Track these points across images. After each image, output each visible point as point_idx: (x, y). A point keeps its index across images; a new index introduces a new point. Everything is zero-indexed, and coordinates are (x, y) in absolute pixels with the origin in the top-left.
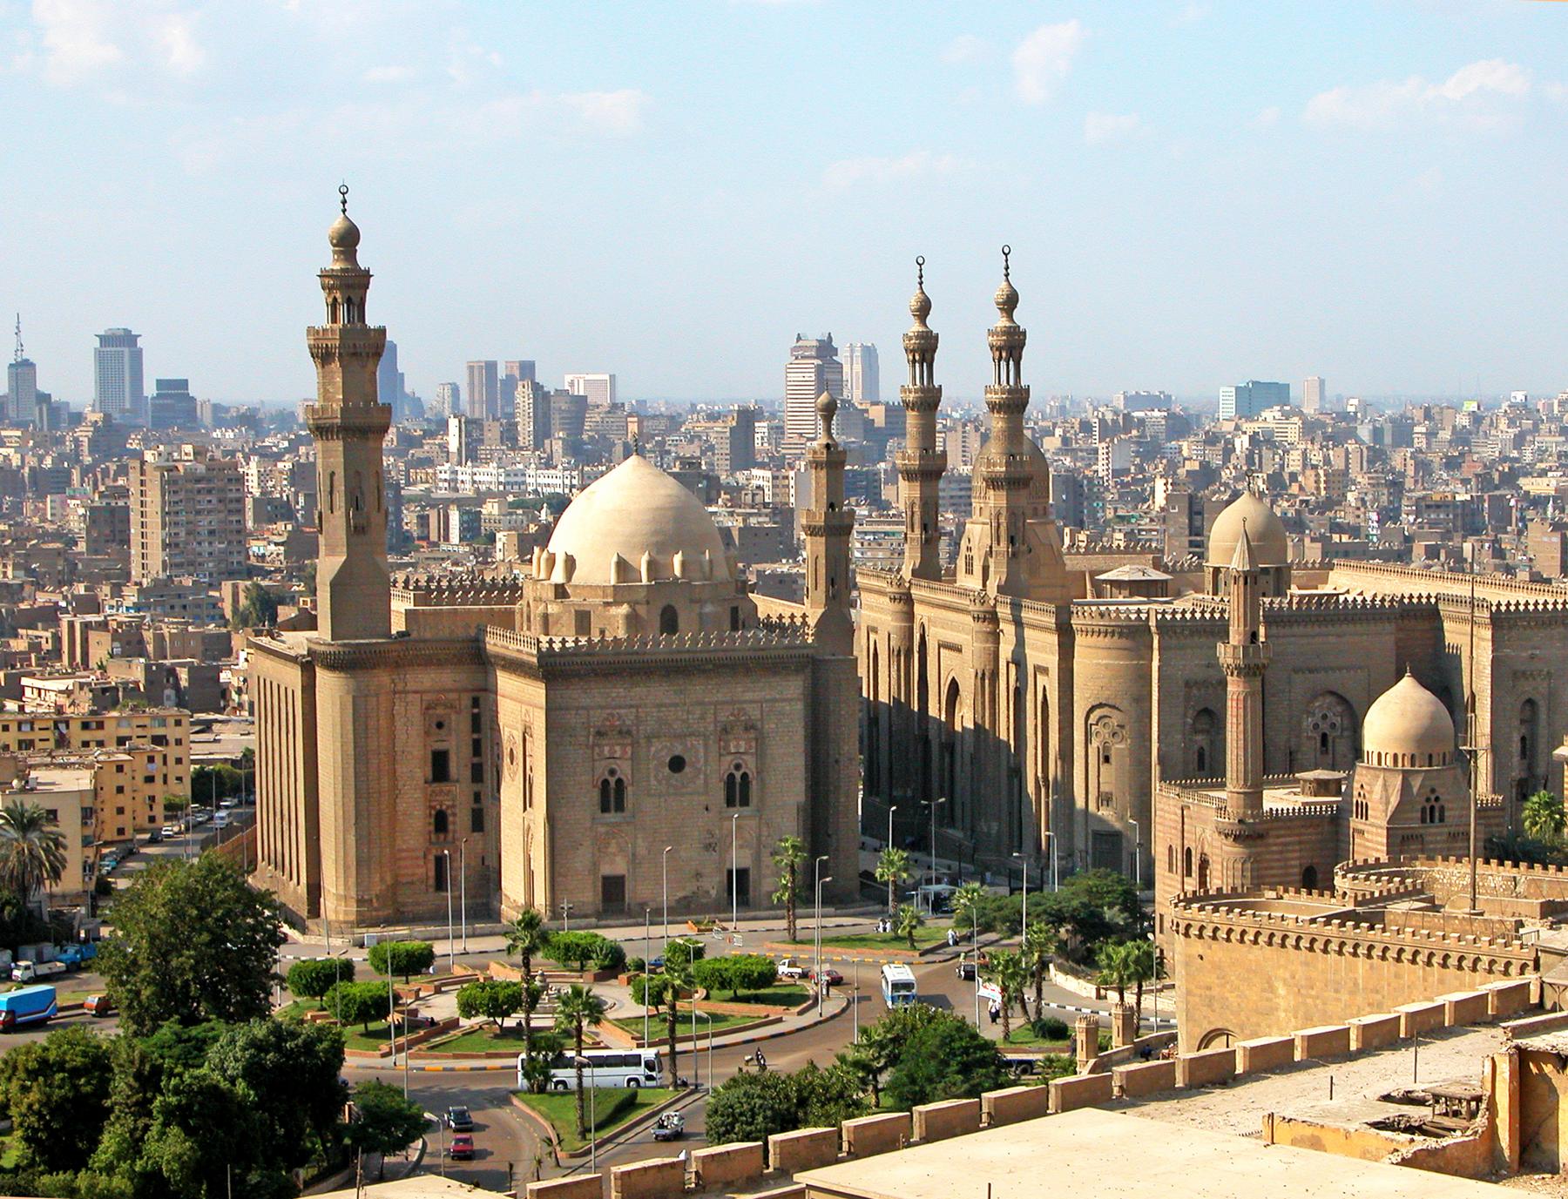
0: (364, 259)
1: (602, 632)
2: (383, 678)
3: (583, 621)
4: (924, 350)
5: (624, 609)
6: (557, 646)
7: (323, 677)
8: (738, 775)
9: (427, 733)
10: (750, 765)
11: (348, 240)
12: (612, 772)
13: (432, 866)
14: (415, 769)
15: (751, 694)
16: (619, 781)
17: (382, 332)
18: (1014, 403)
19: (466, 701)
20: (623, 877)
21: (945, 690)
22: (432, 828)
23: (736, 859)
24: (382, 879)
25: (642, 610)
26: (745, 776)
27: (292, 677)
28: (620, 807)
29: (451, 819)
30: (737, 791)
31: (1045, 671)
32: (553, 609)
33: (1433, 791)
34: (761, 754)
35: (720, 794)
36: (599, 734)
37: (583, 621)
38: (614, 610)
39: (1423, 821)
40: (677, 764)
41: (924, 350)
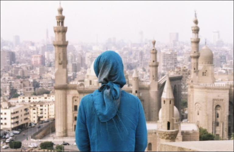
3: (91, 82)
9: (73, 102)
13: (74, 127)
17: (66, 28)
22: (74, 120)
24: (63, 129)
37: (91, 82)
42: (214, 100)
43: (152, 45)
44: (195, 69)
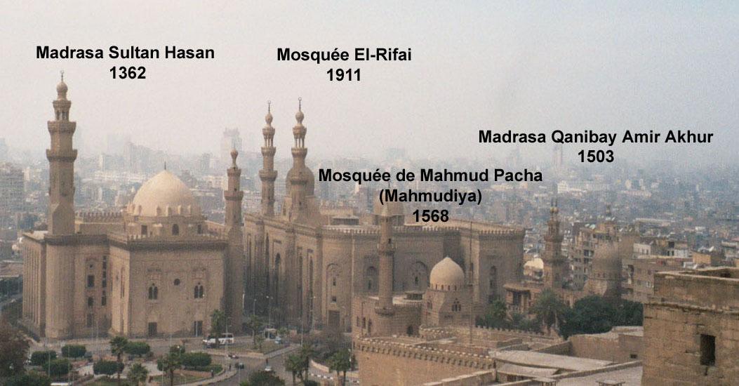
1: (151, 233)
3: (144, 229)
4: (269, 134)
5: (160, 225)
6: (135, 238)
7: (48, 247)
8: (199, 286)
10: (204, 283)
11: (63, 90)
12: (153, 284)
14: (81, 282)
15: (204, 258)
16: (156, 288)
18: (301, 154)
19: (101, 258)
20: (156, 323)
21: (275, 257)
23: (199, 317)
26: (202, 287)
27: (38, 248)
28: (156, 298)
29: (95, 301)
30: (199, 292)
31: (310, 251)
32: (133, 225)
33: (457, 299)
35: (192, 292)
36: (149, 271)
38: (155, 225)
39: (453, 310)
40: (177, 282)
41: (269, 134)
42: (366, 257)
43: (230, 158)
44: (300, 203)
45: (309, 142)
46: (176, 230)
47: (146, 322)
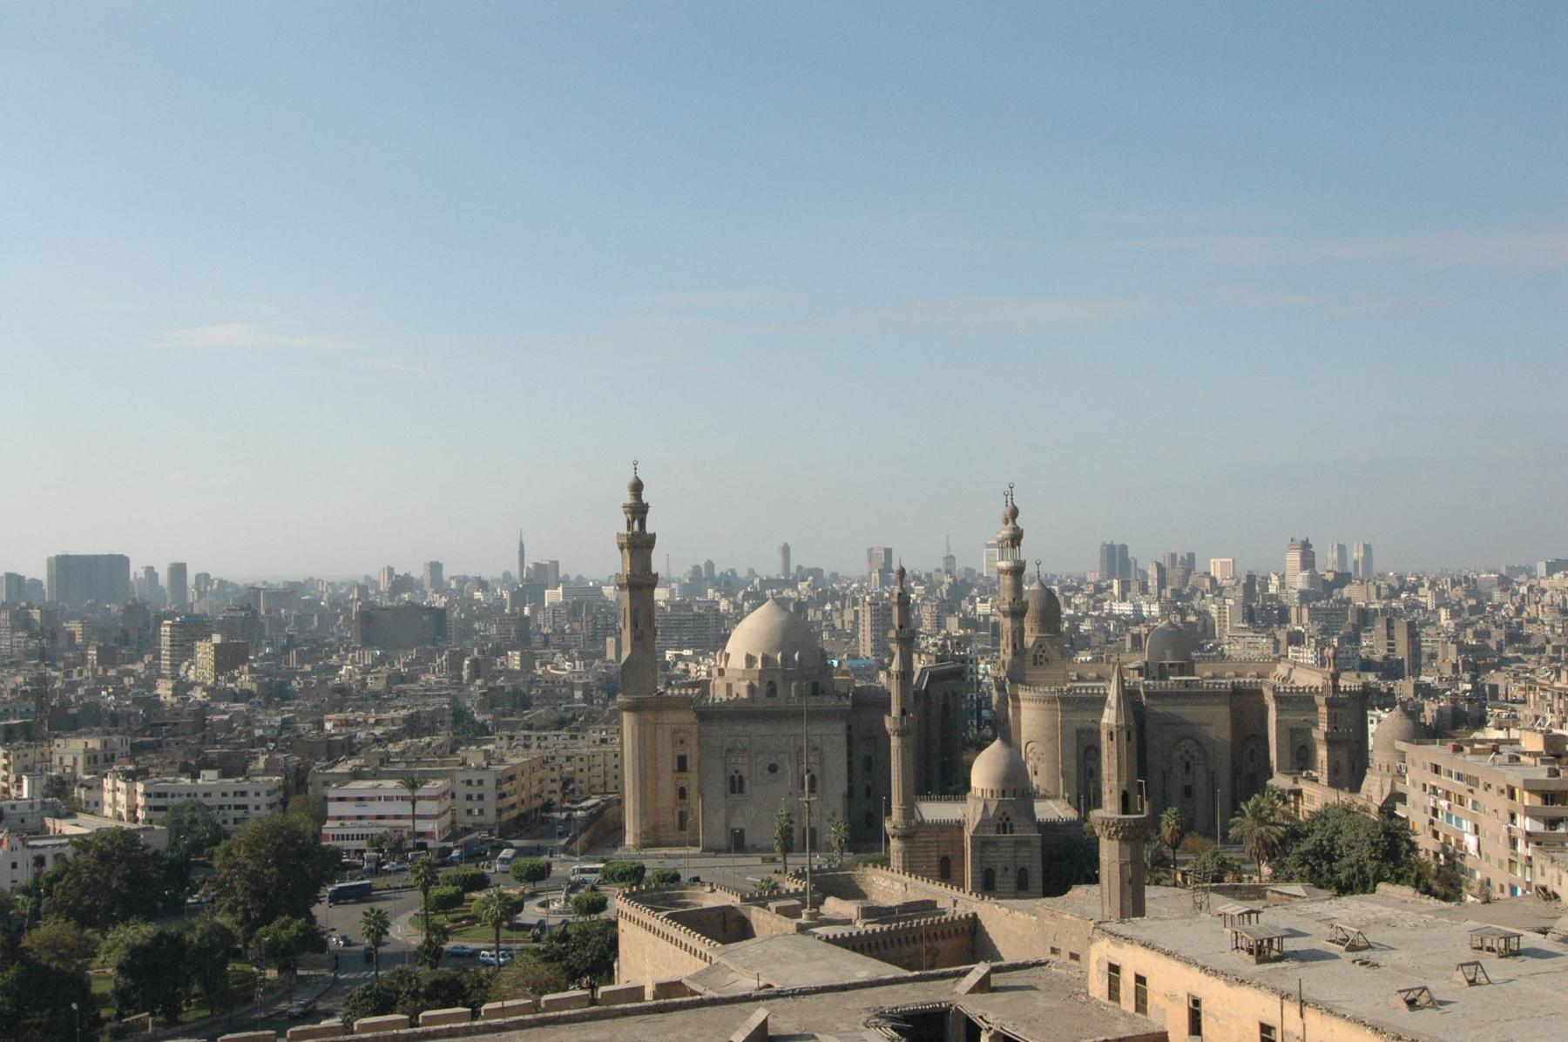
0: (645, 498)
2: (650, 716)
9: (674, 746)
10: (816, 771)
11: (637, 487)
14: (667, 765)
16: (741, 778)
17: (654, 536)
18: (1017, 571)
20: (742, 831)
25: (756, 683)
28: (741, 791)
34: (822, 763)
37: (729, 686)
40: (773, 768)
45: (1028, 551)
46: (772, 690)
47: (727, 827)
